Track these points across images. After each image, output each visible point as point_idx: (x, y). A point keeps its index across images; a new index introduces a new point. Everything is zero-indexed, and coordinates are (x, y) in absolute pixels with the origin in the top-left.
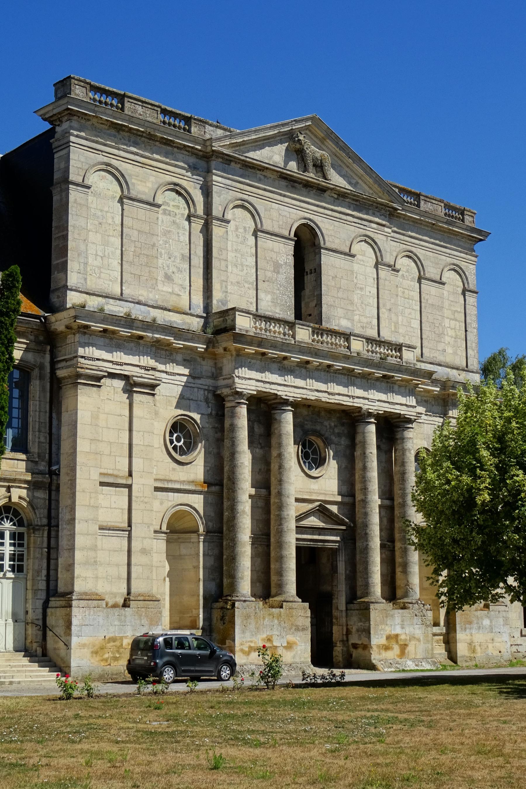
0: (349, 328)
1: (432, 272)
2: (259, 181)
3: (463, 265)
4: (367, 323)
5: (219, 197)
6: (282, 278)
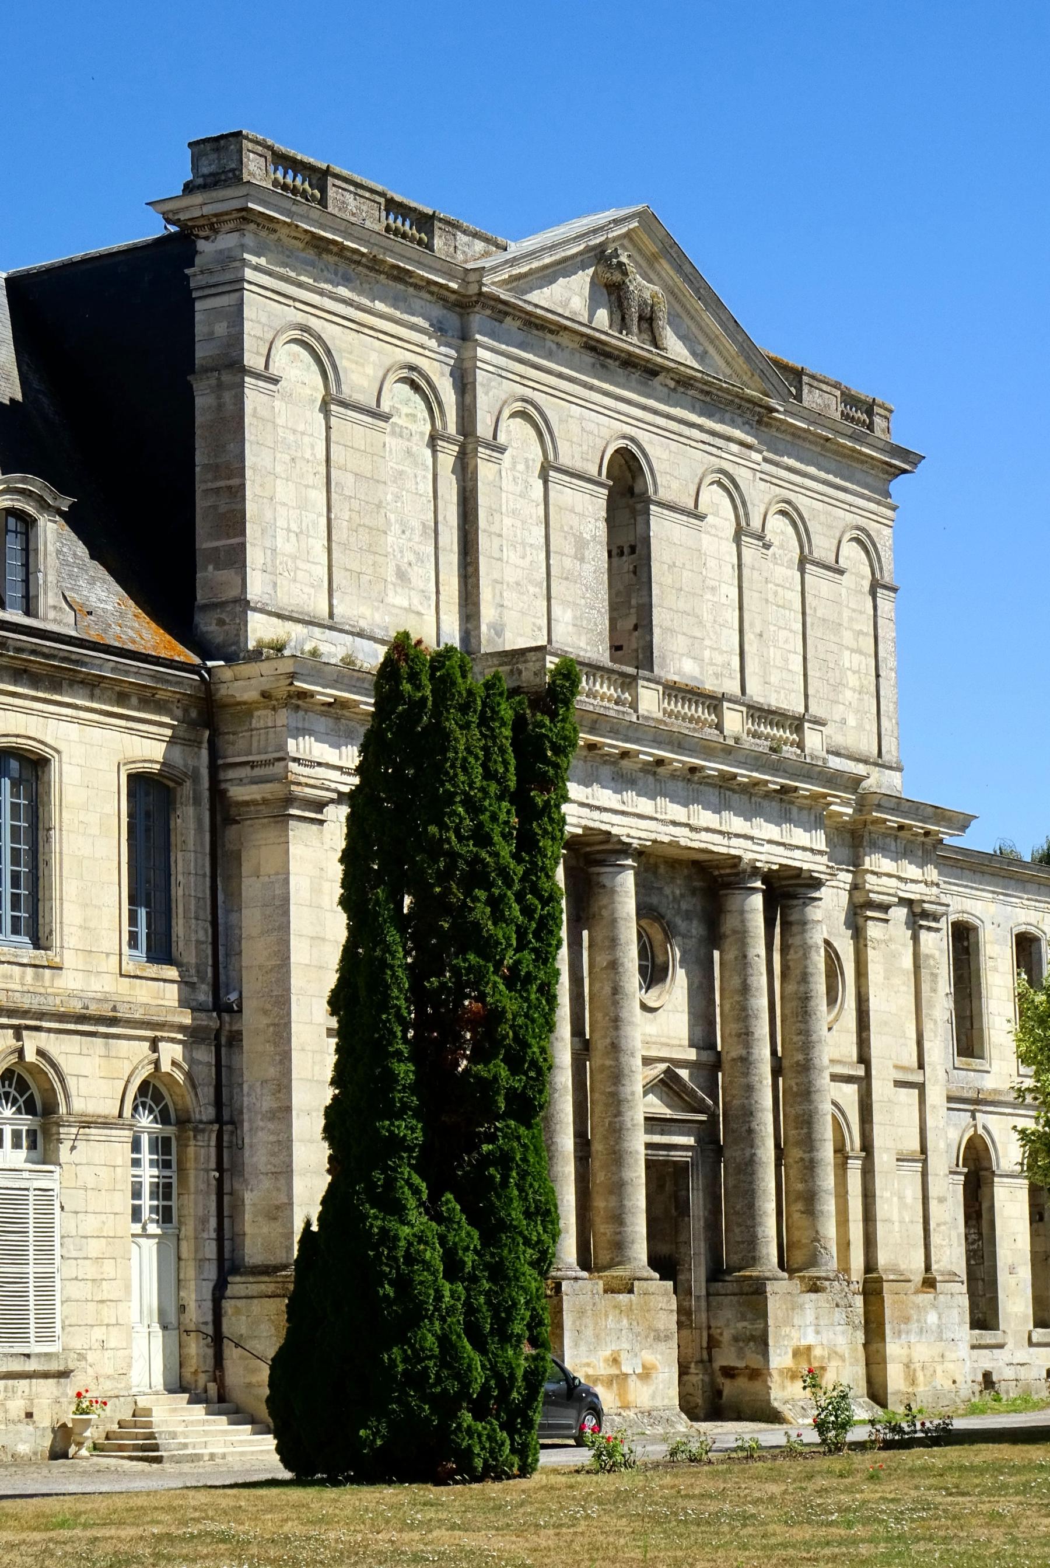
0: (696, 678)
2: (549, 356)
3: (872, 527)
4: (723, 666)
5: (487, 394)
6: (588, 569)
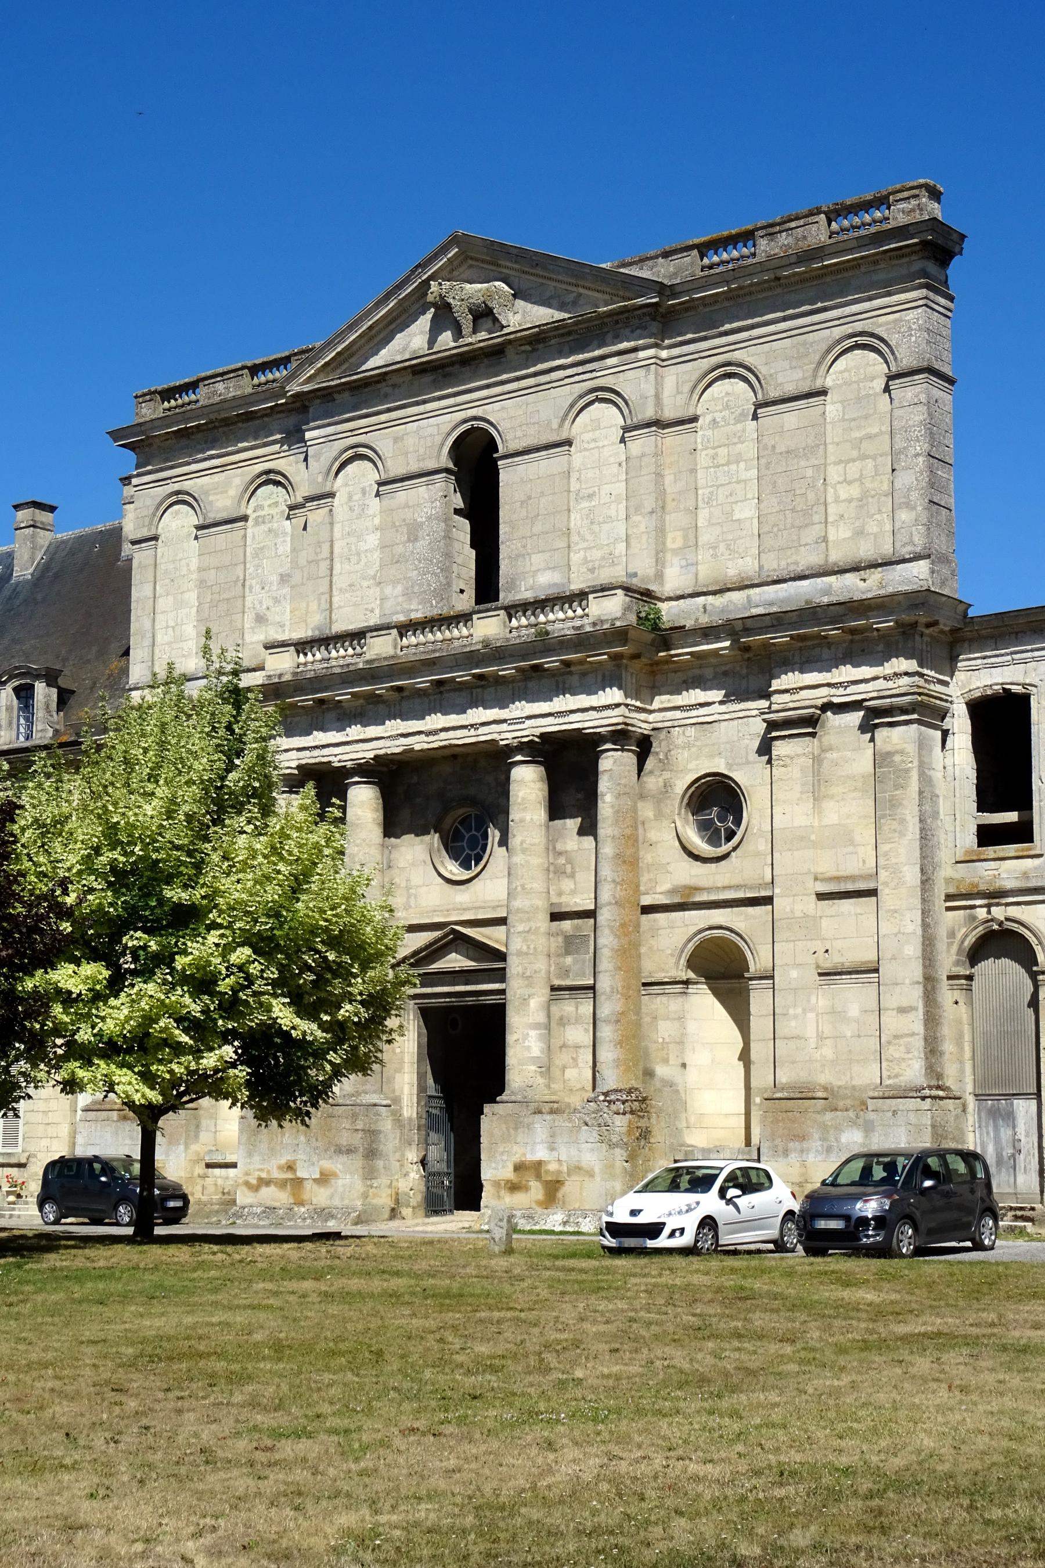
0: (556, 584)
2: (386, 398)
4: (603, 558)
5: (318, 461)
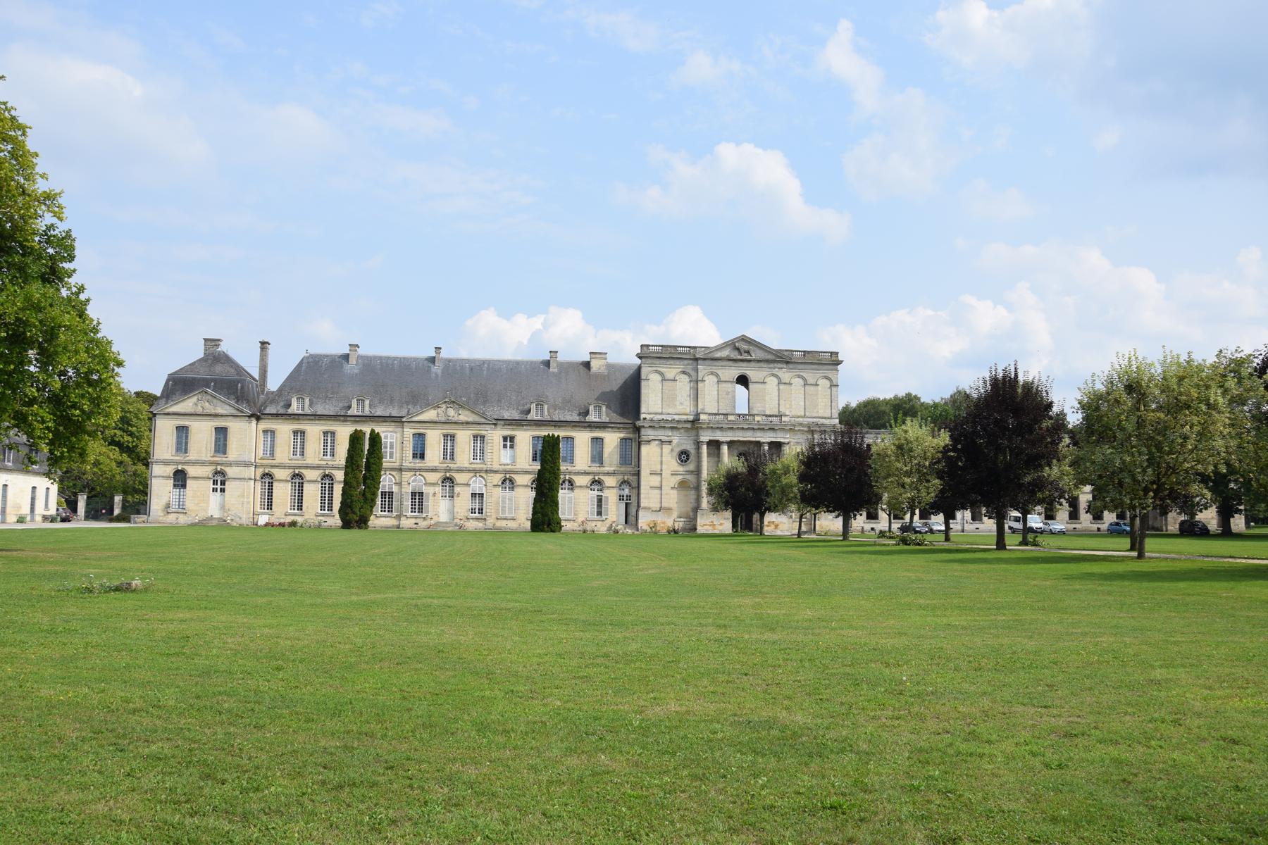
1: (811, 381)
